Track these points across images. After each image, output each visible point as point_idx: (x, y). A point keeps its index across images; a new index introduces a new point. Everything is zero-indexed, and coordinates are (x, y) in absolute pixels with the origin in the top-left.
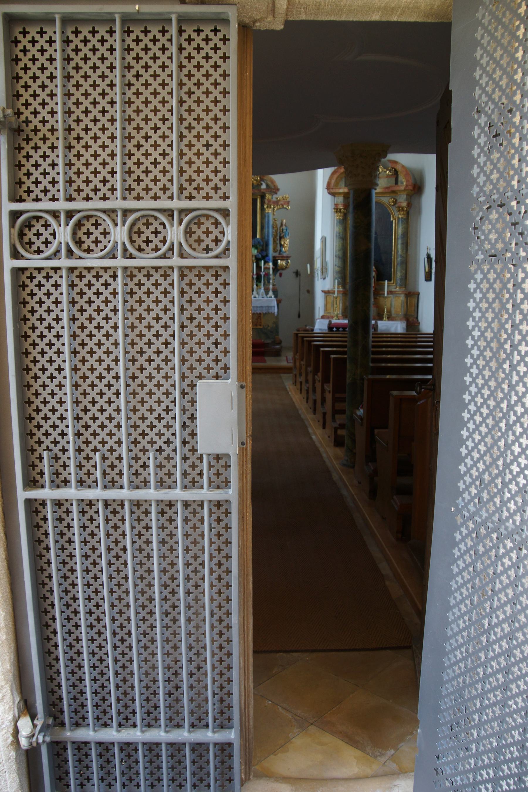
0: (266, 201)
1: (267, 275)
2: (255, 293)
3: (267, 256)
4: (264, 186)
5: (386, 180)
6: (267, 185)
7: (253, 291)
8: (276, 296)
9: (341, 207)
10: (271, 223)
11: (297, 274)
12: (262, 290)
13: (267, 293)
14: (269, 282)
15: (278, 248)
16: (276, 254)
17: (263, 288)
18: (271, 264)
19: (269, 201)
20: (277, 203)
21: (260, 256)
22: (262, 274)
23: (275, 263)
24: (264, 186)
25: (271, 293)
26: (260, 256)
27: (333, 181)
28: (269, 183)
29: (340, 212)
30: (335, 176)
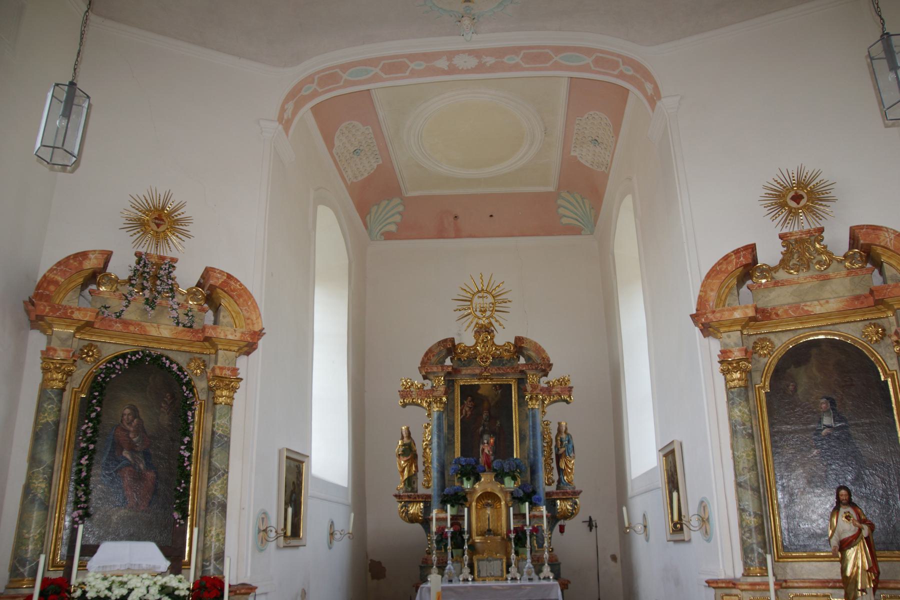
0: (529, 388)
1: (536, 530)
2: (513, 569)
3: (534, 492)
4: (522, 361)
5: (847, 280)
6: (528, 359)
7: (509, 565)
8: (556, 578)
9: (737, 354)
10: (539, 429)
11: (591, 524)
12: (529, 564)
13: (539, 571)
14: (541, 546)
15: (555, 476)
16: (553, 488)
17: (529, 560)
18: (543, 509)
19: (534, 387)
20: (548, 390)
21: (521, 494)
22: (528, 529)
23: (551, 505)
24: (522, 361)
25: (546, 570)
26: (521, 494)
27: (712, 295)
28: (533, 354)
29: (737, 369)
30: (716, 282)
